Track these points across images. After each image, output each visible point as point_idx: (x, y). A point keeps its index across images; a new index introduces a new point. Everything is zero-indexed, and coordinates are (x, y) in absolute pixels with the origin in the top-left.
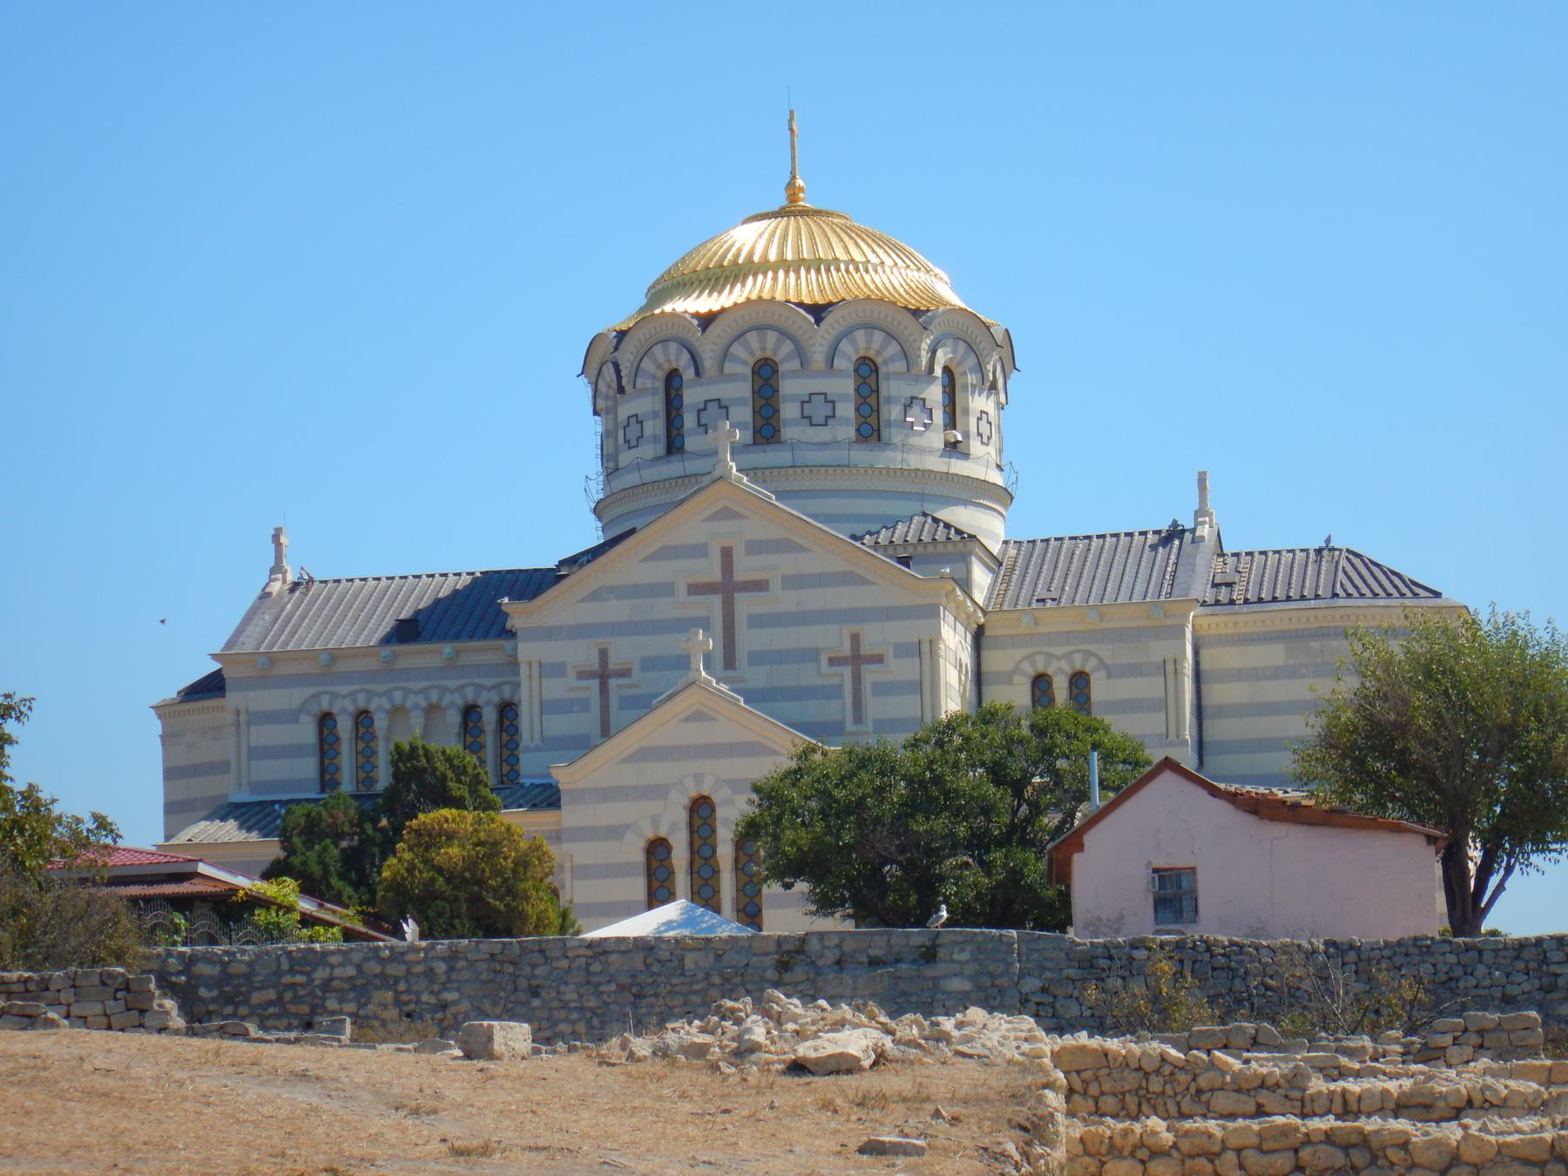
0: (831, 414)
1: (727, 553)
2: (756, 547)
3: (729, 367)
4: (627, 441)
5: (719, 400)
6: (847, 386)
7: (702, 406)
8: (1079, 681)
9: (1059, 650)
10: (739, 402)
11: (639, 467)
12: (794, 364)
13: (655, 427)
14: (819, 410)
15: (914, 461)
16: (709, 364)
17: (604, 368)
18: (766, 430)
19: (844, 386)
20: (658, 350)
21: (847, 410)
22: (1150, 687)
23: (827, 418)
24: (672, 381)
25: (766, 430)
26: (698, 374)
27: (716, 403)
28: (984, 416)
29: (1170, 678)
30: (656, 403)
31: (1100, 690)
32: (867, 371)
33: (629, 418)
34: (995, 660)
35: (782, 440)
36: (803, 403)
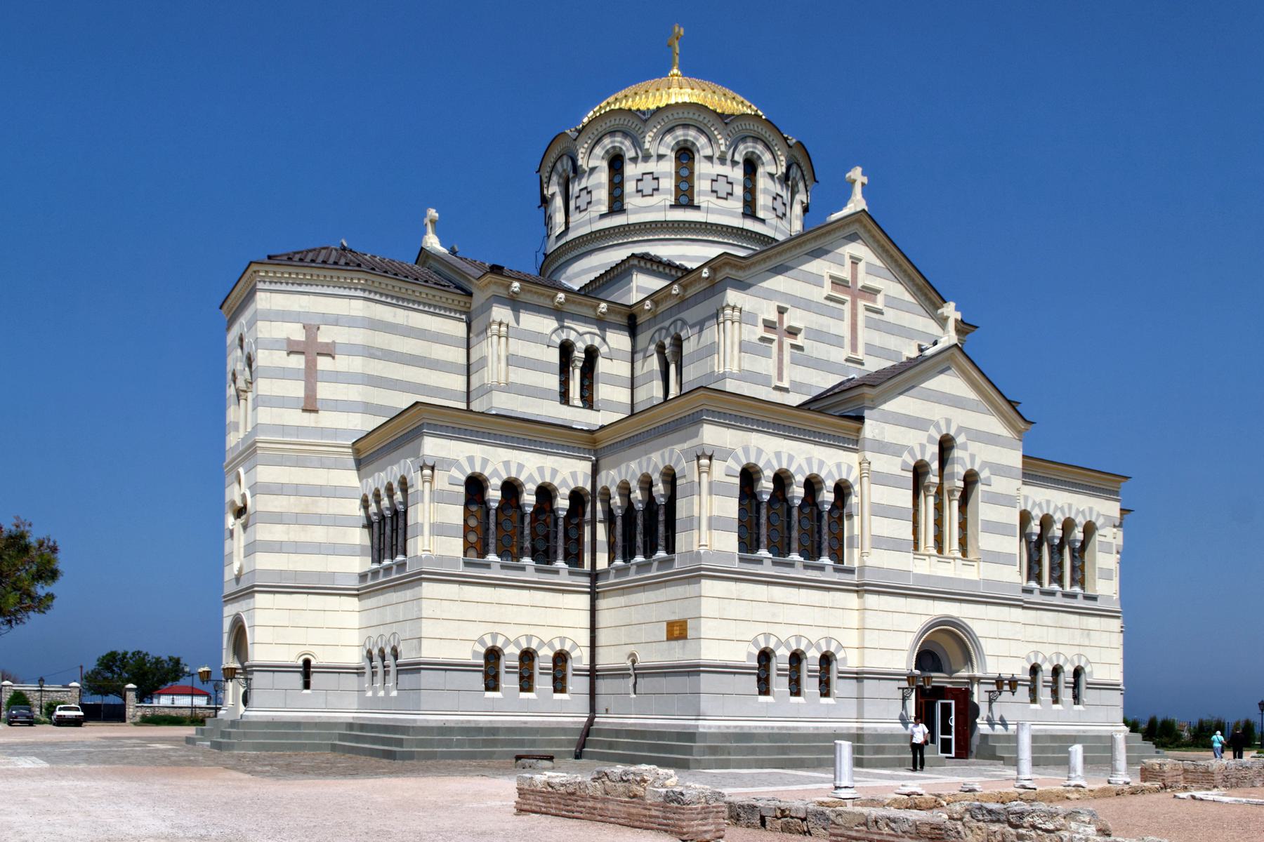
0: (730, 191)
4: (577, 208)
5: (652, 173)
6: (738, 174)
7: (640, 177)
10: (666, 175)
11: (591, 221)
13: (602, 195)
14: (722, 187)
17: (559, 165)
21: (739, 190)
23: (728, 194)
24: (616, 163)
25: (684, 198)
27: (650, 177)
30: (603, 177)
32: (751, 166)
33: (581, 190)
35: (696, 202)
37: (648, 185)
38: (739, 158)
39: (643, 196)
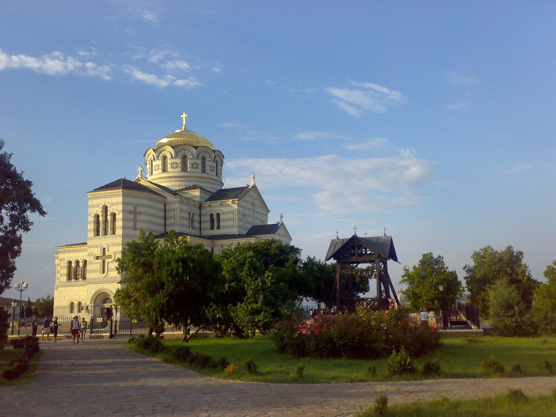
3: (159, 158)
8: (218, 215)
9: (214, 209)
12: (170, 157)
14: (174, 166)
15: (193, 175)
19: (178, 161)
20: (149, 156)
21: (180, 165)
22: (231, 216)
23: (176, 167)
26: (154, 160)
28: (212, 166)
29: (234, 214)
31: (221, 217)
32: (184, 158)
34: (203, 212)
36: (172, 164)
37: (157, 167)
39: (156, 171)
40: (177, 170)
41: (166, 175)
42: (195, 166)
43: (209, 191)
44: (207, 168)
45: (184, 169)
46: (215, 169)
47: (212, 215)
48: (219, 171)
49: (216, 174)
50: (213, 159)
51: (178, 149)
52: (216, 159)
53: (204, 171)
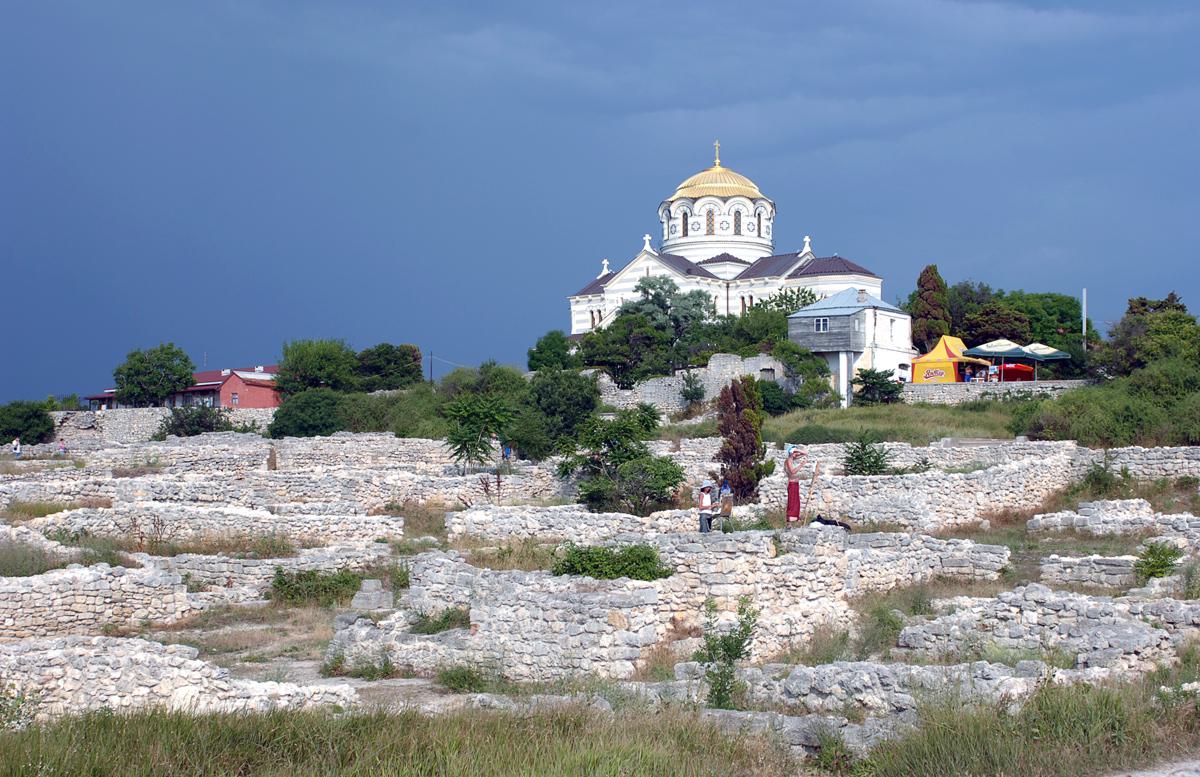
1: (648, 269)
2: (654, 268)
14: (696, 226)
15: (720, 239)
16: (672, 215)
18: (685, 234)
21: (704, 226)
32: (710, 214)
34: (732, 293)
38: (704, 212)
40: (700, 232)
41: (685, 240)
42: (725, 225)
43: (744, 262)
44: (744, 227)
45: (710, 232)
46: (756, 227)
47: (743, 298)
48: (763, 229)
49: (756, 233)
50: (752, 212)
51: (698, 204)
52: (757, 212)
53: (738, 232)
